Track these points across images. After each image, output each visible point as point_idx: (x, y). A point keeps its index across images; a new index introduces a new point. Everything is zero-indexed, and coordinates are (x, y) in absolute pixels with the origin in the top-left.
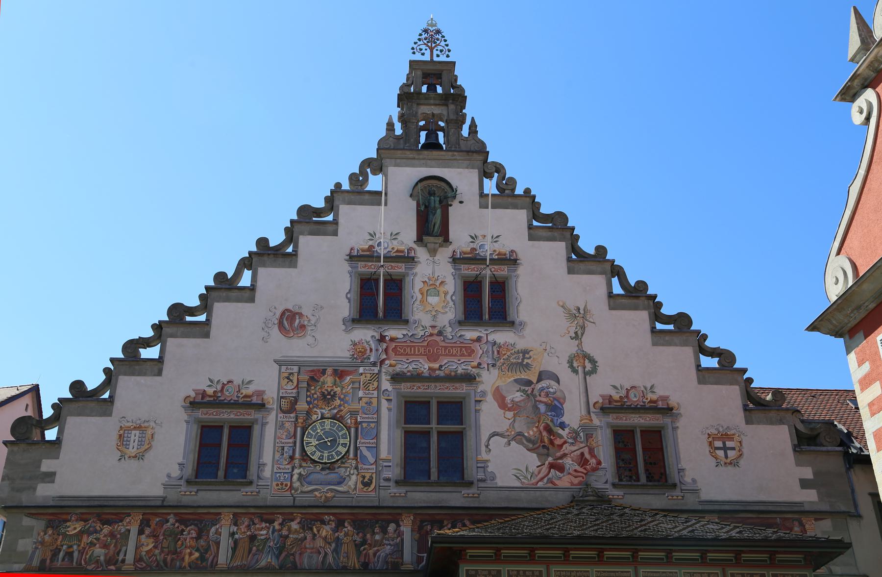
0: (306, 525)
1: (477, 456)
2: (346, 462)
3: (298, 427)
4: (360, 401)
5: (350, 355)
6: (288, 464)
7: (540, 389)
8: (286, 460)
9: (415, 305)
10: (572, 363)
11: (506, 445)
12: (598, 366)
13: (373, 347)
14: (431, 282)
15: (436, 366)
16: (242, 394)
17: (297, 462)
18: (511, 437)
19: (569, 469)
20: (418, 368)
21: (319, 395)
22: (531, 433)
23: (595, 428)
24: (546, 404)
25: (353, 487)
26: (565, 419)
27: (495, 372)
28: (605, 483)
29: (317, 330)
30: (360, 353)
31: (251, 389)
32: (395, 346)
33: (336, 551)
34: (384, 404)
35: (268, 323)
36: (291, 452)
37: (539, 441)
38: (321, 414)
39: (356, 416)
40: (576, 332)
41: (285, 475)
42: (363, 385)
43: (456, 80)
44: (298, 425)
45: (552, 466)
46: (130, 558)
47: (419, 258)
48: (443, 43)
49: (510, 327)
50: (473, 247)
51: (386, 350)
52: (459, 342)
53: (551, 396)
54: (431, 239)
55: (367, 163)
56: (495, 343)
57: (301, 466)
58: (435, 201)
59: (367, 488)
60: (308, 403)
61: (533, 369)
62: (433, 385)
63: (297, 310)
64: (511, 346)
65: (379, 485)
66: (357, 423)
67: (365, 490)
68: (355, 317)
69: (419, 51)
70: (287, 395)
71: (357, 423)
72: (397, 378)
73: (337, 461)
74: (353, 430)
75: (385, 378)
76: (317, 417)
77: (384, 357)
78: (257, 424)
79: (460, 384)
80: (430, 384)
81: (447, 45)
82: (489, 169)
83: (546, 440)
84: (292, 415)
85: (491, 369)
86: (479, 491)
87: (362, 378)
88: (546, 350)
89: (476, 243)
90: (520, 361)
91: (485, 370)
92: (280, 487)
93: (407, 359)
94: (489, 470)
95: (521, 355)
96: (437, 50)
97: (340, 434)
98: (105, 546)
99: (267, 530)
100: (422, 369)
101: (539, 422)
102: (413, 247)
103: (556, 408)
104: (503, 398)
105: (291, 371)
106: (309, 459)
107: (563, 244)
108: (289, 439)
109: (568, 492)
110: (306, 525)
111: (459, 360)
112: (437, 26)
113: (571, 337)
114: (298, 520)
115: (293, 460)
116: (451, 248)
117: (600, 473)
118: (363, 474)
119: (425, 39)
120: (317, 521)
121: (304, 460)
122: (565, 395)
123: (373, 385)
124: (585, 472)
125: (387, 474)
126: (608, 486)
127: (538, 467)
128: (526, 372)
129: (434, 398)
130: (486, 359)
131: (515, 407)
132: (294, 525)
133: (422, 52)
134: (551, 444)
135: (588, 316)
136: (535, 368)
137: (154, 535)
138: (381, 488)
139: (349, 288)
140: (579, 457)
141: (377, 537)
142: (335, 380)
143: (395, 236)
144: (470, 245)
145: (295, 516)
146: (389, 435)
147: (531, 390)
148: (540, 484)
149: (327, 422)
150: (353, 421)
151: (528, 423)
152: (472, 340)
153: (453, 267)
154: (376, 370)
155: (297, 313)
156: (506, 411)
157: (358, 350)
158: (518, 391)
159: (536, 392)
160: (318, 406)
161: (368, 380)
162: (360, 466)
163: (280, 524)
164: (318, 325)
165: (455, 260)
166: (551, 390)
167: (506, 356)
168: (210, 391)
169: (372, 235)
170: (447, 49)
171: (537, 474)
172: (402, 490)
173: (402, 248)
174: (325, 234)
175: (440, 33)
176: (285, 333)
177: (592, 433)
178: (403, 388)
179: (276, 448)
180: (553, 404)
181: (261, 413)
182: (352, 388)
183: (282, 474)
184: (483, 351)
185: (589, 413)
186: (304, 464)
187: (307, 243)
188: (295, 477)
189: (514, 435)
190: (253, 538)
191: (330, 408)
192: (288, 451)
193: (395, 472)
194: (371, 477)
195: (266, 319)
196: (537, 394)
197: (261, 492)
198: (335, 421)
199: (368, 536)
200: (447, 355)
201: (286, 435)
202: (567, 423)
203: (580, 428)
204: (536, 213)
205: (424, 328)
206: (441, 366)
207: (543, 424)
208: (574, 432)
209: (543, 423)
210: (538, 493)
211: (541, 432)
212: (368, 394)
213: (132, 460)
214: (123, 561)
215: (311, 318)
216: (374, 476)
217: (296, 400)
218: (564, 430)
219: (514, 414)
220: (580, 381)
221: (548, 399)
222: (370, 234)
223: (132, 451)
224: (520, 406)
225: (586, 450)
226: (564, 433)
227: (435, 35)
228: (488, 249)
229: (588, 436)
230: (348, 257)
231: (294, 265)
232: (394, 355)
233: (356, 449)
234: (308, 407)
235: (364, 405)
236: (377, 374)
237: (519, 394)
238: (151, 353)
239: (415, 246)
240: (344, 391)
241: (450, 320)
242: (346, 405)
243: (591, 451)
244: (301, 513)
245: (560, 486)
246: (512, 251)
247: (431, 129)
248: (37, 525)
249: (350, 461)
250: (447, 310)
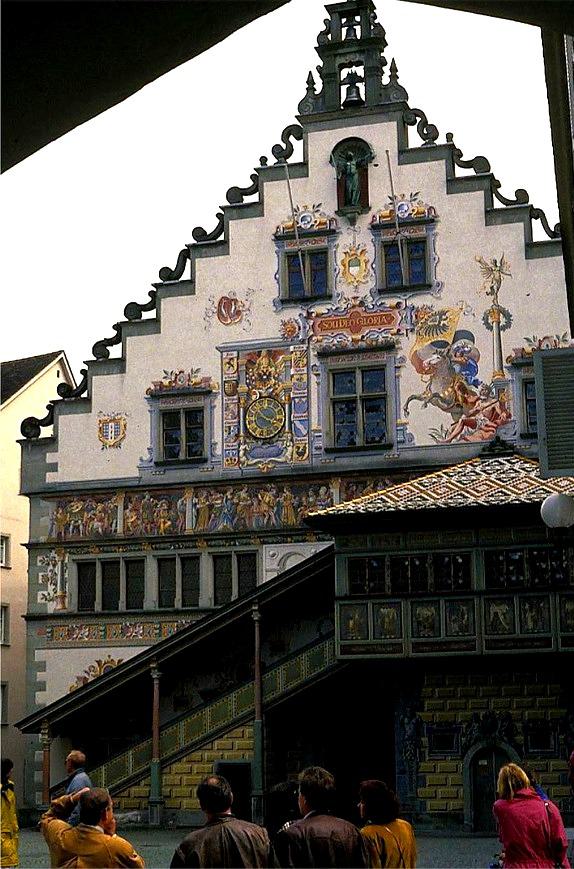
0: (253, 495)
13: (301, 324)
14: (353, 252)
23: (507, 383)
27: (413, 337)
30: (290, 333)
33: (278, 513)
34: (314, 379)
43: (375, 17)
45: (465, 423)
46: (120, 529)
54: (348, 209)
55: (287, 133)
57: (245, 443)
58: (352, 166)
60: (248, 385)
66: (290, 399)
71: (290, 399)
72: (323, 354)
74: (287, 406)
75: (313, 353)
77: (312, 333)
82: (409, 116)
83: (460, 398)
84: (235, 397)
85: (410, 334)
98: (101, 520)
103: (470, 368)
110: (253, 495)
116: (371, 214)
117: (510, 425)
125: (319, 443)
131: (432, 370)
132: (243, 494)
137: (135, 509)
141: (311, 500)
143: (317, 208)
162: (294, 438)
165: (375, 228)
168: (166, 382)
187: (235, 227)
188: (241, 453)
190: (211, 507)
199: (304, 499)
202: (480, 380)
206: (363, 337)
213: (113, 449)
214: (116, 531)
215: (245, 303)
217: (238, 383)
223: (111, 442)
226: (477, 391)
228: (408, 209)
229: (499, 392)
230: (273, 238)
231: (227, 253)
237: (435, 356)
238: (115, 352)
243: (502, 405)
248: (49, 506)
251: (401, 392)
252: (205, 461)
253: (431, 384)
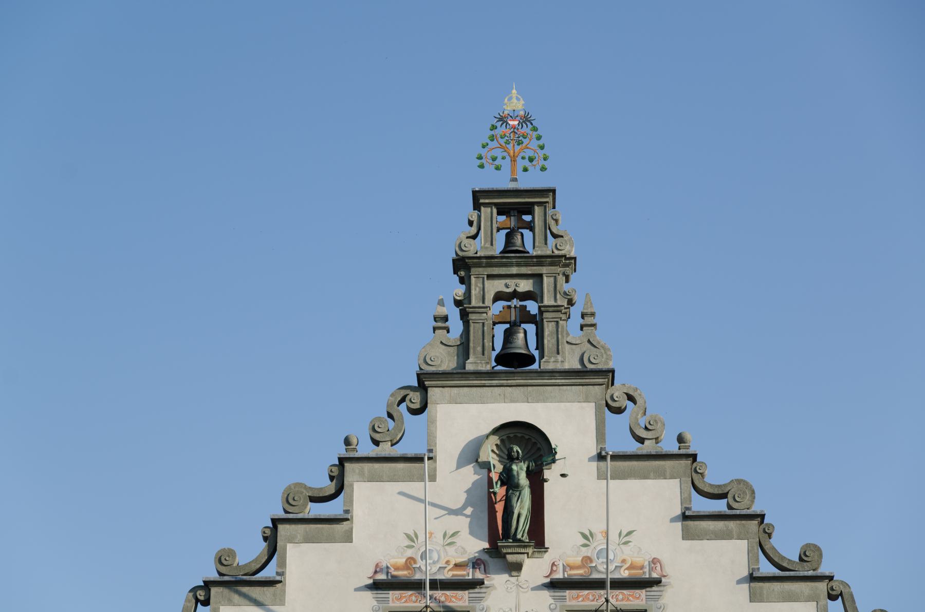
48: (534, 144)
58: (520, 470)
69: (491, 161)
81: (542, 148)
89: (592, 547)
96: (523, 158)
107: (743, 544)
116: (548, 558)
133: (497, 162)
174: (331, 539)
175: (529, 121)
204: (696, 483)
222: (408, 536)
239: (485, 557)
246: (655, 561)
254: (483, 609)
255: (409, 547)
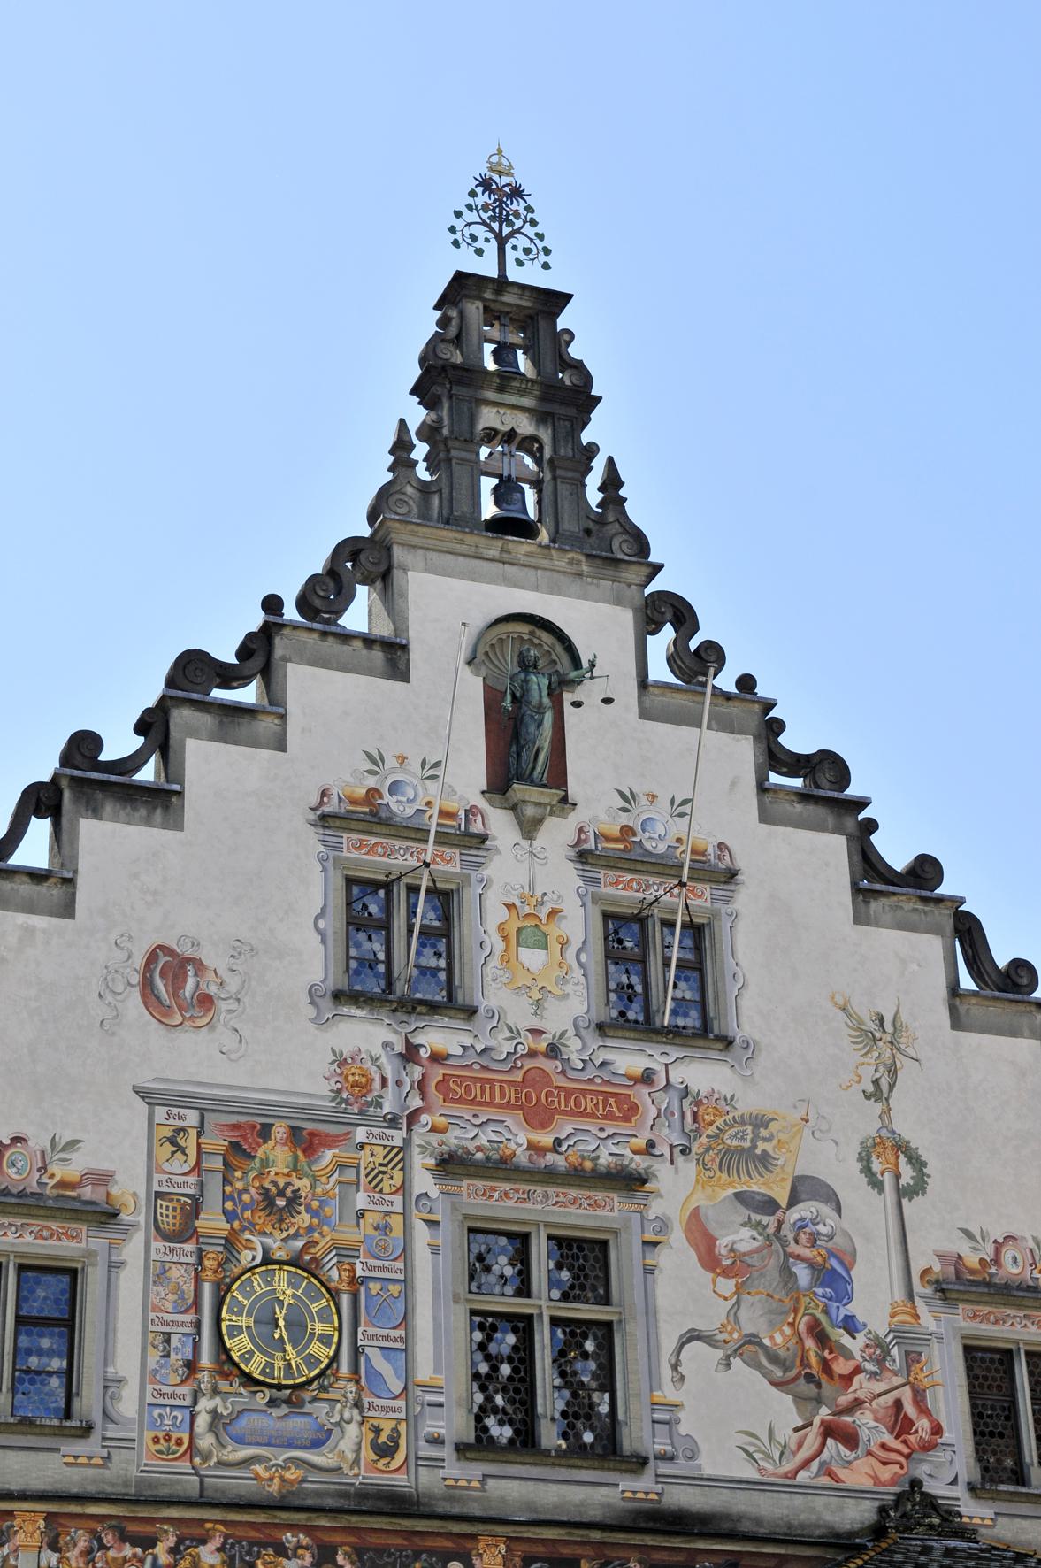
1: (651, 1390)
2: (330, 1386)
3: (203, 1280)
4: (362, 1221)
5: (332, 1091)
6: (183, 1382)
7: (795, 1223)
8: (176, 1371)
9: (489, 970)
10: (869, 1161)
11: (721, 1367)
12: (929, 1176)
13: (389, 1074)
14: (527, 910)
15: (546, 1139)
16: (52, 1176)
17: (204, 1377)
18: (732, 1346)
19: (869, 1441)
20: (501, 1142)
21: (257, 1197)
22: (778, 1339)
23: (926, 1337)
24: (812, 1265)
25: (350, 1456)
26: (855, 1308)
27: (688, 1167)
28: (950, 1484)
29: (243, 1013)
31: (71, 1168)
32: (444, 1075)
34: (421, 1233)
35: (113, 979)
36: (189, 1349)
37: (798, 1363)
38: (263, 1249)
39: (352, 1260)
40: (877, 1080)
41: (174, 1413)
42: (367, 1176)
44: (203, 1275)
45: (829, 1431)
47: (495, 839)
48: (528, 229)
49: (720, 1050)
50: (625, 823)
51: (421, 1085)
52: (600, 1081)
53: (823, 1243)
55: (349, 549)
56: (686, 1092)
57: (215, 1391)
58: (539, 684)
59: (387, 1460)
60: (230, 1216)
61: (778, 1170)
62: (540, 1189)
63: (189, 953)
64: (723, 1103)
65: (416, 1454)
67: (380, 1465)
68: (340, 987)
69: (469, 241)
70: (171, 1190)
71: (355, 1282)
72: (450, 1165)
73: (310, 1382)
74: (345, 1300)
76: (254, 1258)
78: (94, 1265)
79: (606, 1194)
80: (532, 1188)
83: (813, 1360)
84: (189, 1247)
85: (679, 1159)
86: (660, 1485)
87: (364, 1156)
88: (807, 1121)
89: (635, 812)
90: (747, 1144)
91: (664, 1162)
92: (162, 1445)
93: (475, 1116)
94: (683, 1429)
95: (749, 1129)
97: (314, 1307)
99: (138, 1564)
100: (512, 1146)
101: (796, 1311)
102: (479, 806)
104: (711, 1241)
105: (180, 1123)
106: (235, 1371)
108: (181, 1313)
109: (867, 1502)
111: (602, 1130)
112: (511, 175)
113: (864, 1092)
114: (217, 1541)
115: (195, 1373)
117: (940, 1456)
118: (376, 1422)
119: (485, 208)
120: (265, 1545)
121: (226, 1376)
122: (855, 1249)
123: (392, 1178)
124: (906, 1451)
125: (434, 1425)
126: (960, 1491)
127: (796, 1430)
128: (762, 1176)
129: (542, 1228)
130: (666, 1131)
133: (478, 244)
134: (826, 1373)
135: (904, 1040)
136: (782, 1167)
138: (420, 1462)
139: (320, 904)
140: (890, 1412)
142: (296, 1159)
144: (620, 817)
145: (208, 1530)
146: (435, 1318)
147: (776, 1225)
148: (803, 1477)
149: (281, 1277)
150: (345, 1274)
151: (770, 1311)
152: (630, 1078)
153: (581, 873)
154: (398, 1137)
155: (189, 960)
156: (719, 1275)
157: (351, 1078)
158: (744, 1225)
159: (787, 1231)
160: (254, 1225)
161: (380, 1165)
162: (366, 1400)
163: (174, 1551)
164: (246, 1000)
166: (821, 1228)
167: (713, 1128)
169: (376, 760)
170: (540, 248)
171: (793, 1446)
172: (475, 1470)
173: (451, 806)
176: (159, 1013)
177: (919, 1349)
178: (465, 1193)
179: (150, 1336)
180: (827, 1266)
181: (103, 1235)
182: (340, 1182)
183: (168, 1409)
184: (659, 1110)
185: (910, 1296)
186: (224, 1386)
188: (202, 1421)
189: (739, 1340)
191: (285, 1234)
192: (180, 1346)
193: (454, 1423)
194: (395, 1430)
195: (106, 967)
196: (791, 1237)
197: (115, 1458)
198: (299, 1271)
200: (570, 1113)
201: (175, 1302)
202: (861, 1318)
203: (891, 1335)
205: (514, 1033)
206: (558, 1142)
207: (806, 1319)
208: (877, 1346)
209: (804, 1315)
210: (798, 1500)
211: (800, 1339)
212: (380, 1203)
216: (403, 1428)
217: (195, 1206)
218: (854, 1338)
219: (736, 1285)
220: (889, 1211)
221: (816, 1253)
224: (749, 1266)
225: (906, 1395)
226: (855, 1345)
227: (509, 202)
232: (441, 1100)
233: (356, 1351)
234: (228, 1226)
235: (371, 1232)
236: (401, 1149)
237: (746, 1233)
239: (482, 803)
240: (319, 1190)
241: (576, 1018)
242: (325, 1228)
243: (919, 1397)
244: (223, 1523)
245: (849, 1483)
247: (505, 474)
249: (341, 1384)
250: (569, 988)
251: (662, 1316)
252: (86, 1431)
253: (738, 1303)
254: (482, 880)
255: (370, 772)
